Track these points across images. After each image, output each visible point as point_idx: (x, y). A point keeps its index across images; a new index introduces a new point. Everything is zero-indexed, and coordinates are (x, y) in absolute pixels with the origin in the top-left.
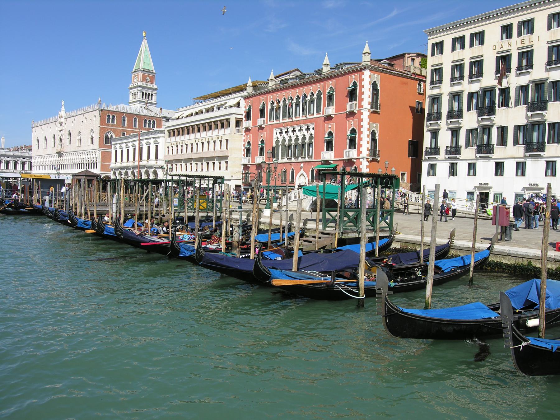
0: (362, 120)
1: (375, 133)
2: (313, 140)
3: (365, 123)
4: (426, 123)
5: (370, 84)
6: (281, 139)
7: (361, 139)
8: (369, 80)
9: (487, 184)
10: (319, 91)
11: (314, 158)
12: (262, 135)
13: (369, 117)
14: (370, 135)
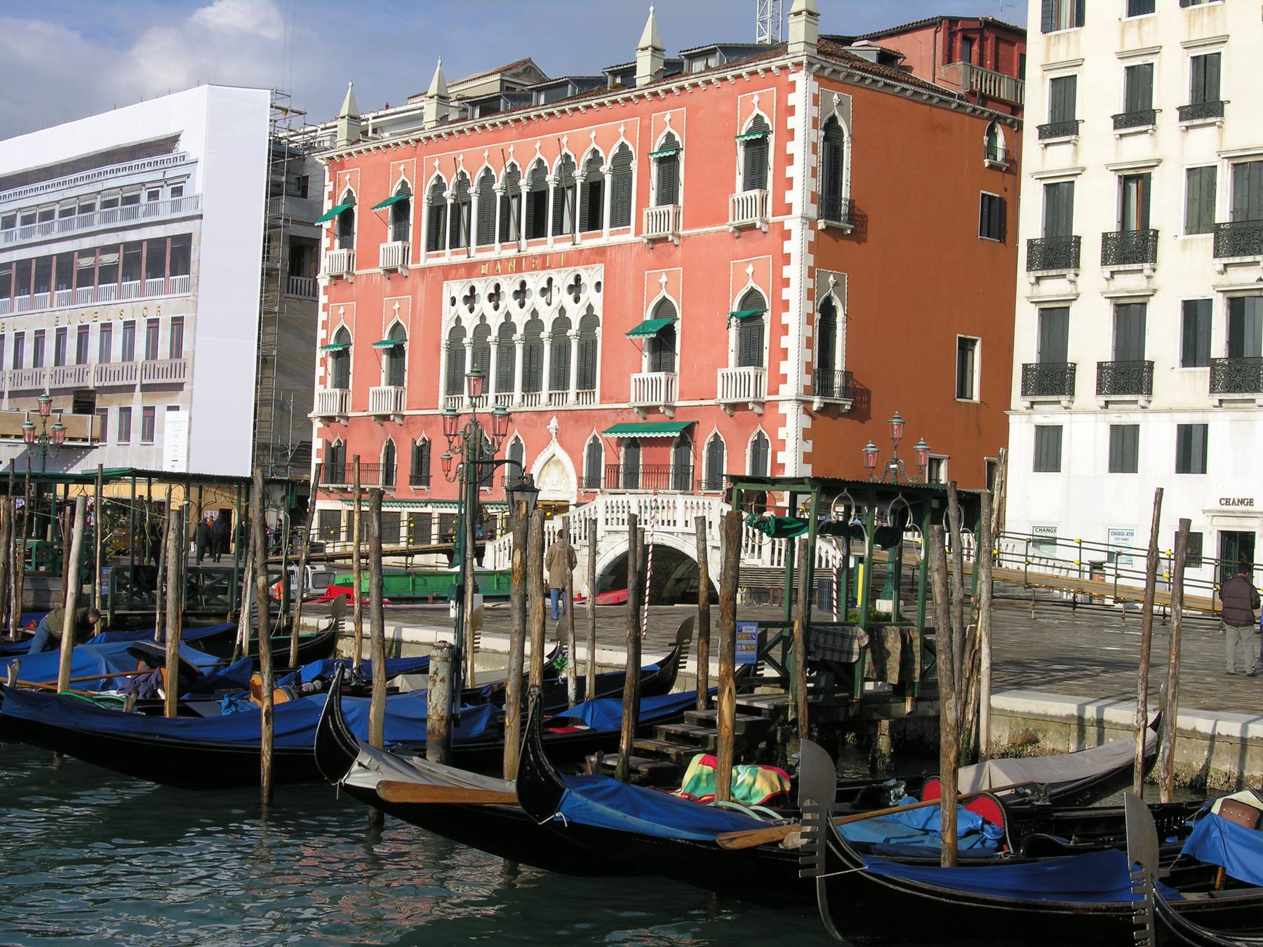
0: (787, 259)
1: (834, 309)
2: (599, 331)
3: (795, 272)
4: (1024, 278)
5: (815, 126)
6: (470, 322)
8: (815, 112)
9: (1251, 502)
10: (623, 147)
11: (603, 399)
13: (813, 248)
14: (818, 316)
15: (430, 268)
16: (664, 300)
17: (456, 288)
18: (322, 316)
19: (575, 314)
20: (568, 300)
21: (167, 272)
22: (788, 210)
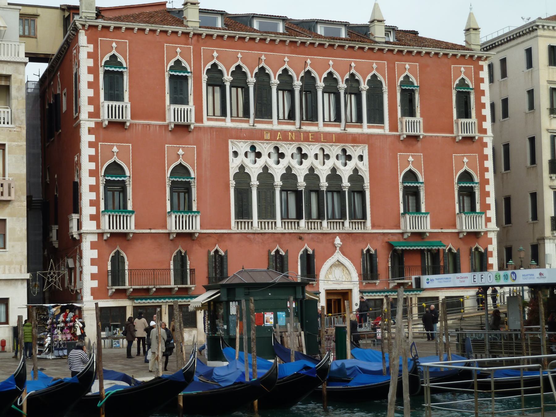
0: (486, 157)
6: (254, 170)
11: (373, 226)
12: (181, 153)
15: (211, 128)
16: (410, 171)
17: (243, 147)
18: (86, 152)
19: (345, 172)
20: (294, 163)
22: (484, 131)
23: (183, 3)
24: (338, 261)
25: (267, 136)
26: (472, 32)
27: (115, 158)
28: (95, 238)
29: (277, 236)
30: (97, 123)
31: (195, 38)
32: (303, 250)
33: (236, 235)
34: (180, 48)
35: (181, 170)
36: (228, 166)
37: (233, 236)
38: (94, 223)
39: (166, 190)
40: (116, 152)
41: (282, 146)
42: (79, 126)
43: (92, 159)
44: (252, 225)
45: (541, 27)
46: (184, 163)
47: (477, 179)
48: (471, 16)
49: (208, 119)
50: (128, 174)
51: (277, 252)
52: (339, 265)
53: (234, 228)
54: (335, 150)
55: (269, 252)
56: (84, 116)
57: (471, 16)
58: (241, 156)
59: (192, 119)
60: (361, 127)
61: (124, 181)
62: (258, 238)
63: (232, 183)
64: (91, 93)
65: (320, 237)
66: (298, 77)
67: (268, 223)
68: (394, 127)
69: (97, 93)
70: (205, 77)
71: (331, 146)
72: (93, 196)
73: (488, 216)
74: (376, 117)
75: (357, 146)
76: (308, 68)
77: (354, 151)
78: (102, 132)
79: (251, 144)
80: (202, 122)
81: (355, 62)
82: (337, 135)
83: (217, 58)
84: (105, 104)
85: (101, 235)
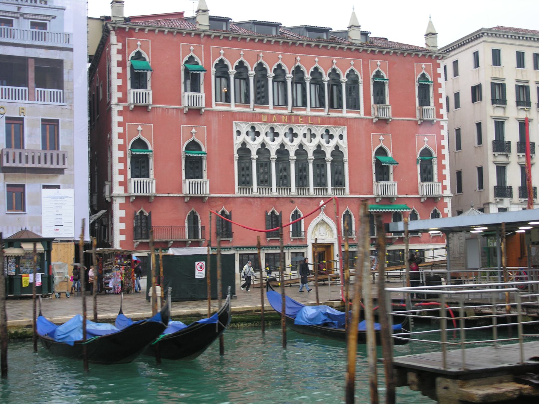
0: (443, 137)
6: (254, 146)
7: (441, 167)
11: (351, 192)
15: (220, 111)
17: (245, 127)
18: (116, 130)
19: (328, 148)
21: (32, 83)
22: (441, 116)
23: (196, 10)
24: (322, 220)
25: (265, 119)
26: (431, 36)
27: (140, 136)
28: (123, 201)
29: (272, 199)
30: (124, 107)
31: (206, 38)
32: (294, 211)
33: (239, 199)
34: (194, 46)
35: (194, 146)
36: (233, 143)
37: (237, 199)
38: (123, 187)
39: (181, 162)
40: (142, 130)
41: (276, 127)
42: (110, 110)
43: (120, 136)
44: (252, 191)
45: (486, 34)
46: (197, 140)
47: (435, 155)
48: (430, 24)
49: (216, 105)
50: (150, 148)
51: (273, 212)
52: (323, 223)
53: (237, 193)
54: (319, 131)
55: (266, 212)
56: (114, 101)
57: (430, 24)
58: (243, 135)
59: (203, 103)
60: (341, 112)
61: (147, 155)
62: (258, 201)
63: (236, 156)
64: (120, 82)
65: (308, 200)
66: (289, 71)
67: (266, 189)
68: (368, 112)
69: (125, 82)
70: (213, 70)
71: (317, 127)
72: (121, 166)
73: (444, 184)
74: (353, 104)
75: (339, 128)
76: (298, 64)
77: (336, 132)
78: (129, 114)
79: (252, 125)
80: (211, 107)
81: (336, 59)
82: (322, 117)
83: (224, 55)
84: (131, 92)
85: (128, 198)
